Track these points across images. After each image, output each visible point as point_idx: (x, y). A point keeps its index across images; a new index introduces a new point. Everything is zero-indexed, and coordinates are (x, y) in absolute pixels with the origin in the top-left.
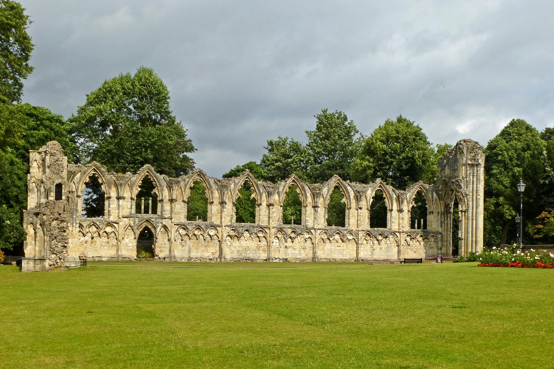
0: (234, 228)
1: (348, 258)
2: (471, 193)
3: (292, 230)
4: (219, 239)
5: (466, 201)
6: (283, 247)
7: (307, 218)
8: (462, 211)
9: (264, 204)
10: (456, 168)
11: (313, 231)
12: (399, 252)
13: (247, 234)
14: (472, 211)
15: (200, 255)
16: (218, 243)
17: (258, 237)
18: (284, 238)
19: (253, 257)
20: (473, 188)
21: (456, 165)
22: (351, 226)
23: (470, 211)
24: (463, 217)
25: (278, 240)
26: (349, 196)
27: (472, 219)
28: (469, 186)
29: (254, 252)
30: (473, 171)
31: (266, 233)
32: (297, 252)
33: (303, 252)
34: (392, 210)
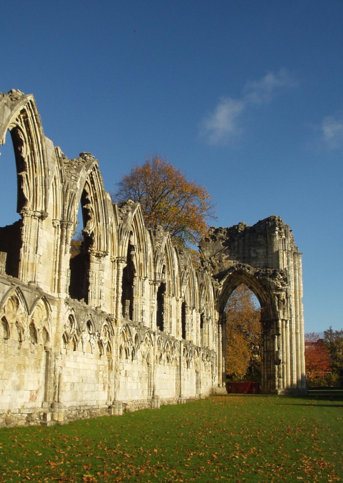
0: (73, 313)
2: (294, 294)
4: (50, 344)
5: (289, 305)
6: (123, 373)
8: (283, 320)
11: (152, 335)
13: (85, 335)
14: (296, 322)
15: (8, 400)
16: (44, 354)
20: (295, 287)
21: (255, 251)
23: (293, 319)
24: (284, 329)
26: (174, 271)
27: (297, 333)
28: (291, 284)
30: (294, 262)
32: (135, 387)
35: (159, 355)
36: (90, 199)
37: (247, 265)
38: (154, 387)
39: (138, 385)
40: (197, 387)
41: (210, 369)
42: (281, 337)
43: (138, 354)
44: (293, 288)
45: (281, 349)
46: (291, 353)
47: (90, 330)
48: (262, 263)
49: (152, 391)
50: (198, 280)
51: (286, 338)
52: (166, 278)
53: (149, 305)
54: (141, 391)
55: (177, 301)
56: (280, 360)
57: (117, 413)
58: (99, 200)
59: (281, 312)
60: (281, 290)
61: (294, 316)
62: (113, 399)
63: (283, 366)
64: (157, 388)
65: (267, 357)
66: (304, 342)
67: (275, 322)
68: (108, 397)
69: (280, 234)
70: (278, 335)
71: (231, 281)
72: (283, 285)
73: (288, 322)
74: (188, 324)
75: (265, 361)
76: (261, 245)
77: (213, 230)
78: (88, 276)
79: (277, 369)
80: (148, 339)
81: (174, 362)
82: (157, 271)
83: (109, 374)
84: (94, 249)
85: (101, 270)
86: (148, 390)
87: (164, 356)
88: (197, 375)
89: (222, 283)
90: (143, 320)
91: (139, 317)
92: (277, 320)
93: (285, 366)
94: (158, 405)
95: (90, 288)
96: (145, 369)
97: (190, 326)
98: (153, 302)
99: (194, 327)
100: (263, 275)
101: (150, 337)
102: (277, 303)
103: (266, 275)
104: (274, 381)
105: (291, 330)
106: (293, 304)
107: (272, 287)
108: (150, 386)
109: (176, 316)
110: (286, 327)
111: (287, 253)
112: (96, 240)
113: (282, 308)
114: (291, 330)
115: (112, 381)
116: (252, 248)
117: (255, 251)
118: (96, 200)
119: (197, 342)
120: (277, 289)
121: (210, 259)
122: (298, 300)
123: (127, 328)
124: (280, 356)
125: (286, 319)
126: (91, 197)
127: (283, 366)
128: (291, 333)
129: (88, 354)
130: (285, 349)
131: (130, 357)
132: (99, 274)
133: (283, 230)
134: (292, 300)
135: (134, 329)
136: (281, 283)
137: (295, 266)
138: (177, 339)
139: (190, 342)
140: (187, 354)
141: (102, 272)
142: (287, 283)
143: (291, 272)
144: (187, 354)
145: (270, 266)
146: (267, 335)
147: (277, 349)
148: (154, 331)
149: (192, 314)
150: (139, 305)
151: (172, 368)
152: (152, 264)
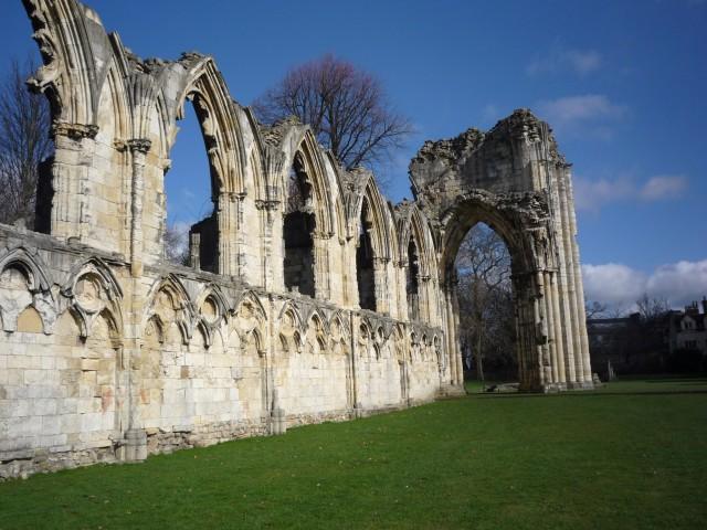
1: (334, 408)
3: (208, 292)
5: (554, 247)
6: (174, 371)
7: (244, 249)
8: (545, 272)
9: (106, 135)
10: (492, 175)
11: (264, 300)
12: (405, 380)
14: (568, 273)
17: (76, 313)
18: (182, 328)
19: (46, 443)
20: (563, 218)
21: (494, 168)
22: (332, 294)
24: (549, 287)
25: (155, 337)
26: (329, 194)
27: (570, 292)
29: (52, 406)
30: (559, 179)
31: (119, 292)
32: (219, 396)
33: (234, 393)
34: (387, 260)
35: (289, 334)
36: (41, 17)
37: (481, 191)
38: (273, 395)
39: (227, 395)
40: (403, 389)
41: (435, 357)
42: (543, 300)
43: (226, 336)
44: (558, 219)
45: (545, 319)
46: (563, 325)
47: (29, 283)
48: (507, 184)
49: (270, 402)
50: (393, 216)
51: (553, 301)
52: (313, 205)
53: (258, 245)
54: (240, 403)
55: (342, 244)
56: (545, 337)
57: (132, 457)
58: (63, 20)
59: (541, 259)
60: (539, 225)
61: (564, 265)
62: (125, 427)
63: (550, 347)
64: (281, 392)
65: (525, 334)
66: (583, 306)
67: (532, 277)
68: (116, 422)
69: (531, 136)
70: (540, 296)
71: (461, 218)
72: (541, 216)
73: (555, 275)
74: (380, 286)
75: (523, 340)
76: (503, 158)
77: (430, 145)
78: (52, 177)
79: (541, 353)
80: (254, 305)
81: (339, 347)
82: (271, 184)
83: (117, 377)
84: (62, 121)
85: (82, 164)
86: (263, 399)
87: (309, 336)
88: (402, 369)
89: (445, 222)
90: (242, 273)
91: (234, 266)
92: (535, 273)
93: (554, 346)
94: (284, 426)
95: (55, 200)
96: (251, 361)
97: (383, 288)
98: (267, 239)
99: (392, 291)
100: (507, 202)
101: (258, 301)
102: (533, 246)
103: (513, 202)
104: (538, 372)
105: (560, 287)
106: (561, 245)
107: (524, 220)
108: (265, 394)
109: (340, 270)
110: (551, 283)
111: (546, 166)
112: (66, 103)
113: (542, 251)
114: (560, 287)
115: (123, 388)
116: (489, 165)
117: (494, 168)
118: (57, 20)
119: (400, 315)
120: (532, 223)
121: (427, 188)
122: (569, 239)
123: (176, 284)
124: (545, 332)
125: (550, 270)
126: (44, 14)
127: (550, 347)
128: (561, 293)
129: (29, 335)
130: (551, 318)
131: (197, 337)
132: (79, 172)
133: (535, 129)
134: (559, 239)
135: (202, 285)
136: (538, 212)
137: (560, 185)
138: (344, 308)
139: (384, 315)
140: (373, 334)
141: (84, 167)
142: (547, 212)
143: (555, 195)
144: (373, 334)
145: (519, 188)
146: (522, 299)
147: (538, 321)
148: (269, 290)
149: (385, 269)
150: (233, 246)
151: (336, 358)
152: (260, 172)
